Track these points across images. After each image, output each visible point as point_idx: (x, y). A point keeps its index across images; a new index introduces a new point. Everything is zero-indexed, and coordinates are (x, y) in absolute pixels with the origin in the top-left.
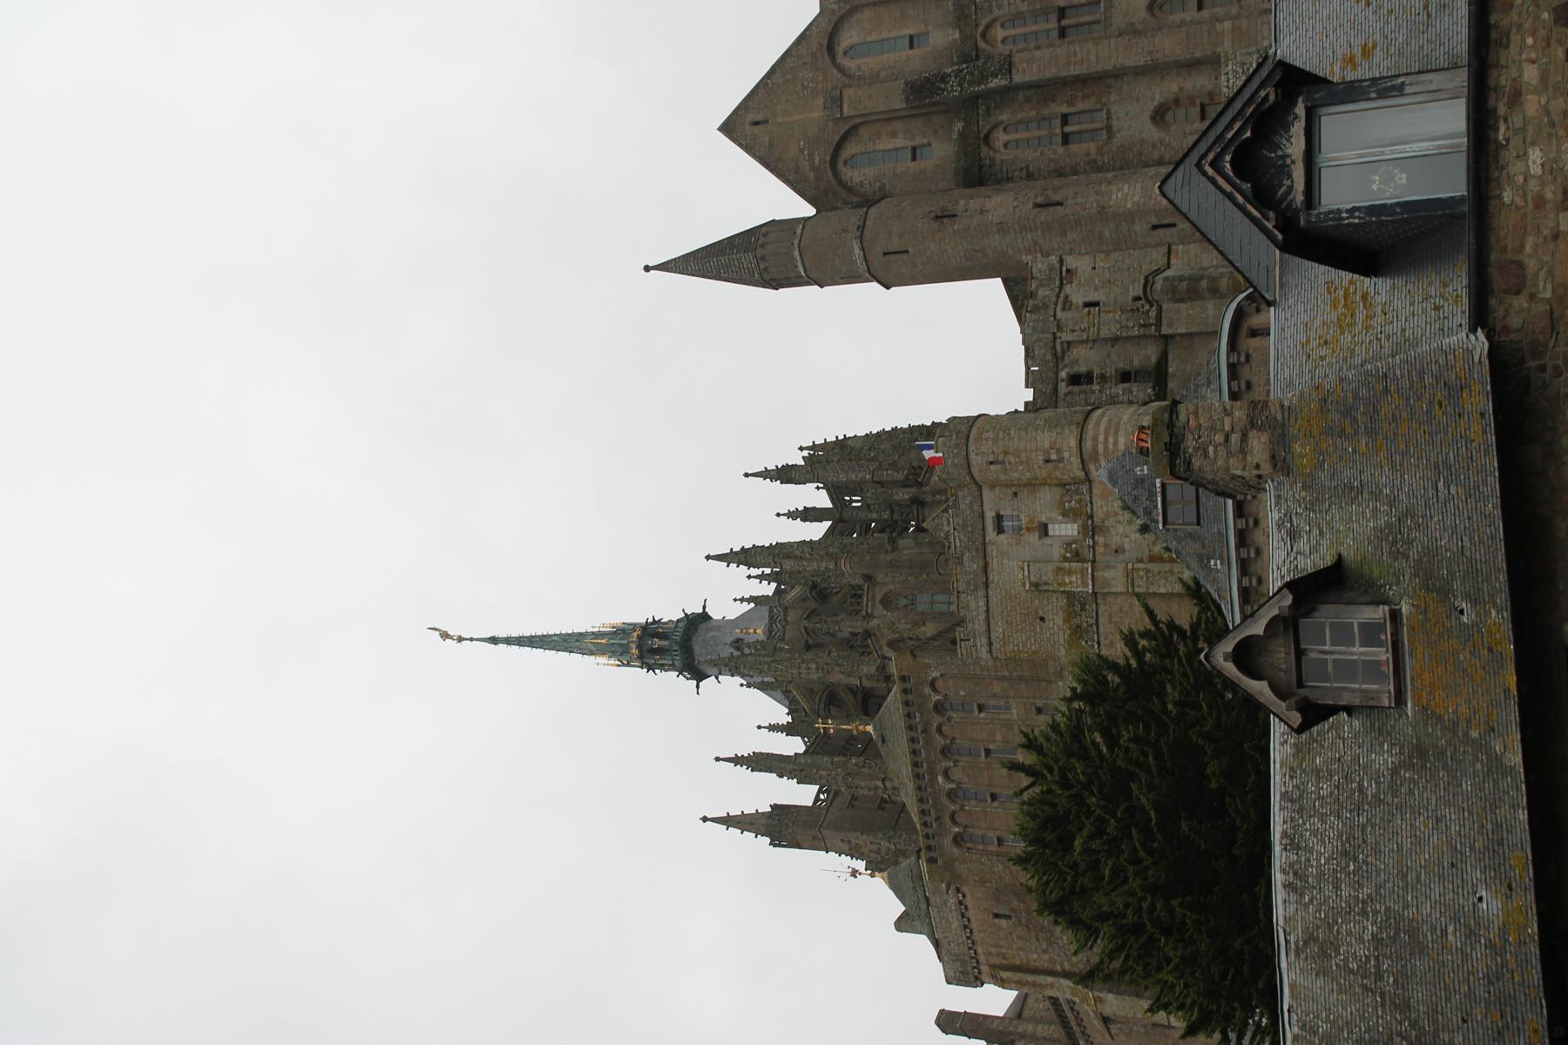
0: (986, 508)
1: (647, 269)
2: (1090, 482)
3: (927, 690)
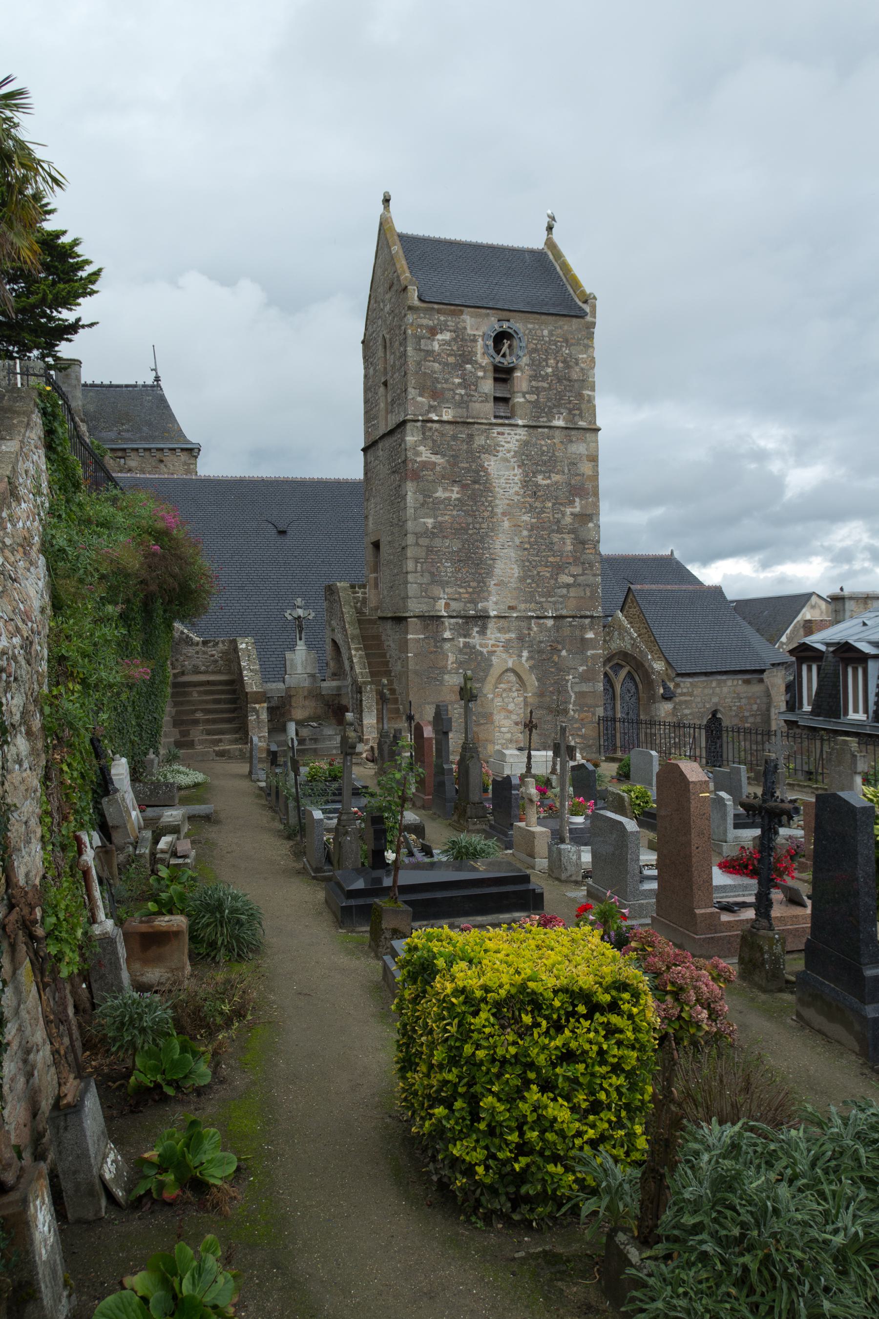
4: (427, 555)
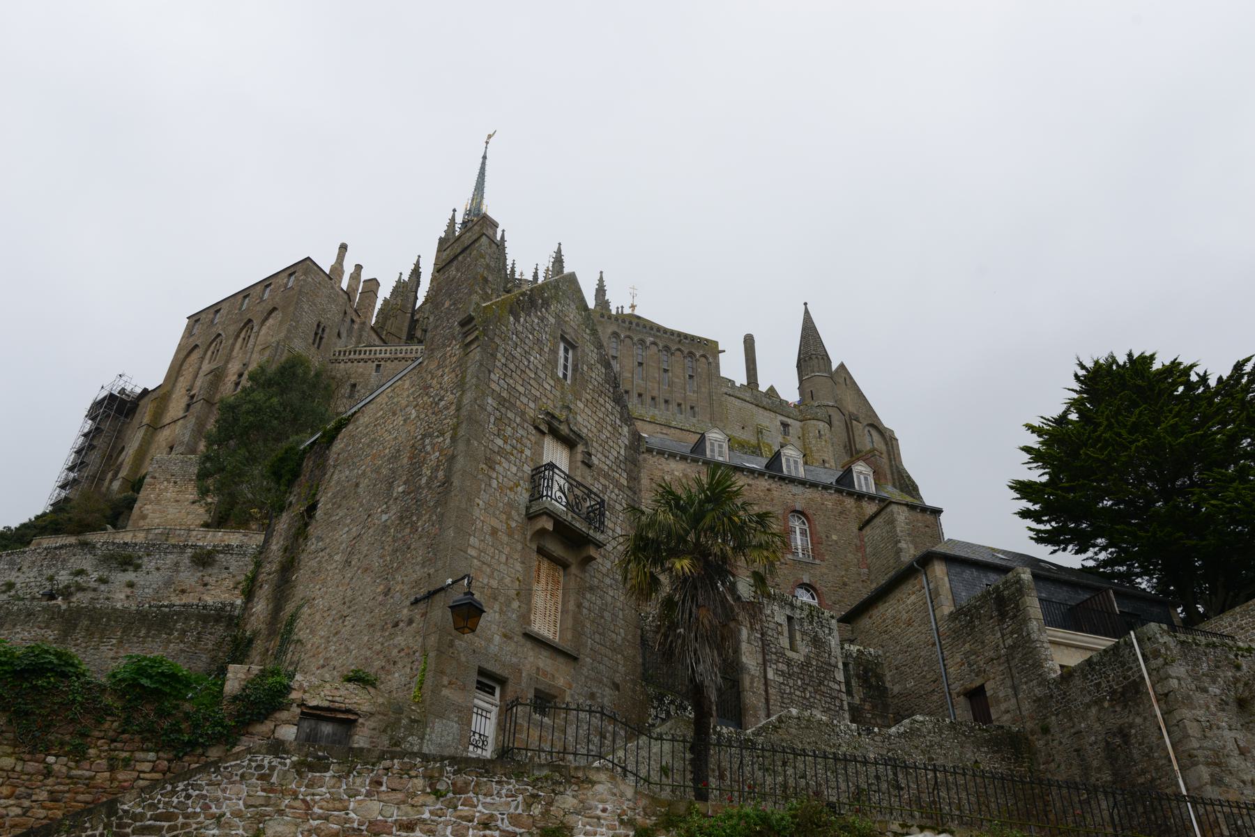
0: (792, 420)
1: (805, 304)
3: (702, 352)
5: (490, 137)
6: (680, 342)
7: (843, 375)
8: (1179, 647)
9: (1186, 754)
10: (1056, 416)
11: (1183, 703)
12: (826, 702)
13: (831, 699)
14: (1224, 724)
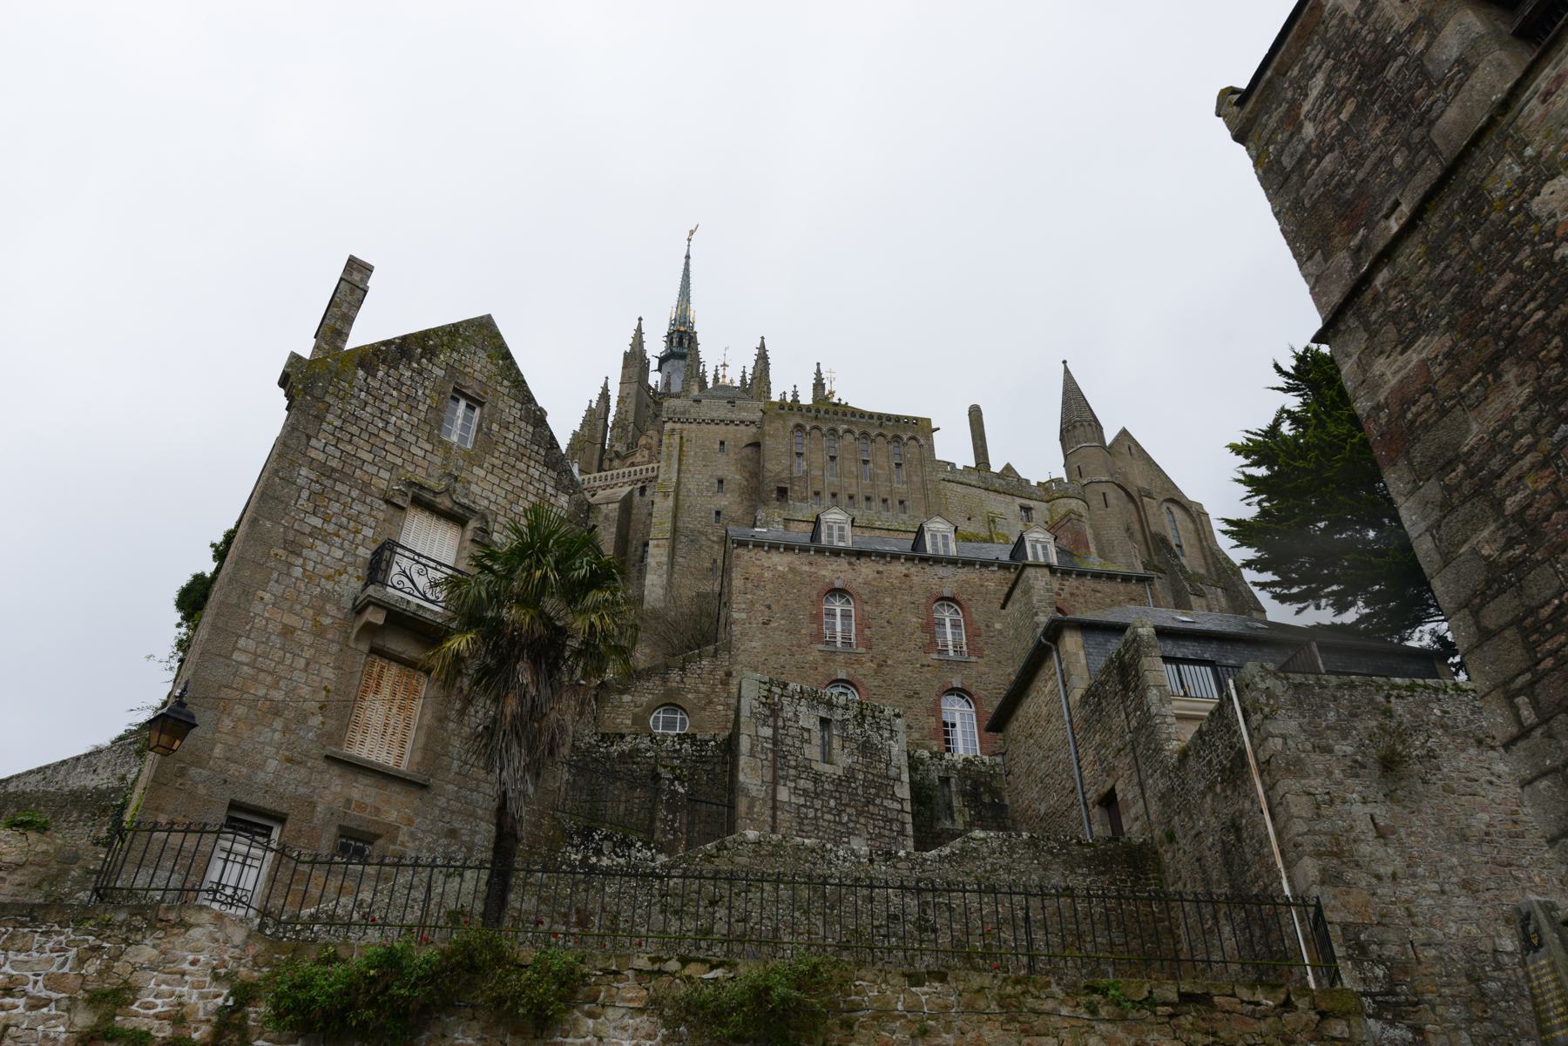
1: (1065, 362)
2: (1066, 573)
3: (910, 434)
4: (1531, 648)
5: (692, 233)
6: (881, 425)
7: (1127, 443)
8: (1290, 692)
9: (1291, 844)
10: (1265, 428)
11: (1288, 770)
12: (875, 826)
13: (885, 822)
14: (1354, 795)
